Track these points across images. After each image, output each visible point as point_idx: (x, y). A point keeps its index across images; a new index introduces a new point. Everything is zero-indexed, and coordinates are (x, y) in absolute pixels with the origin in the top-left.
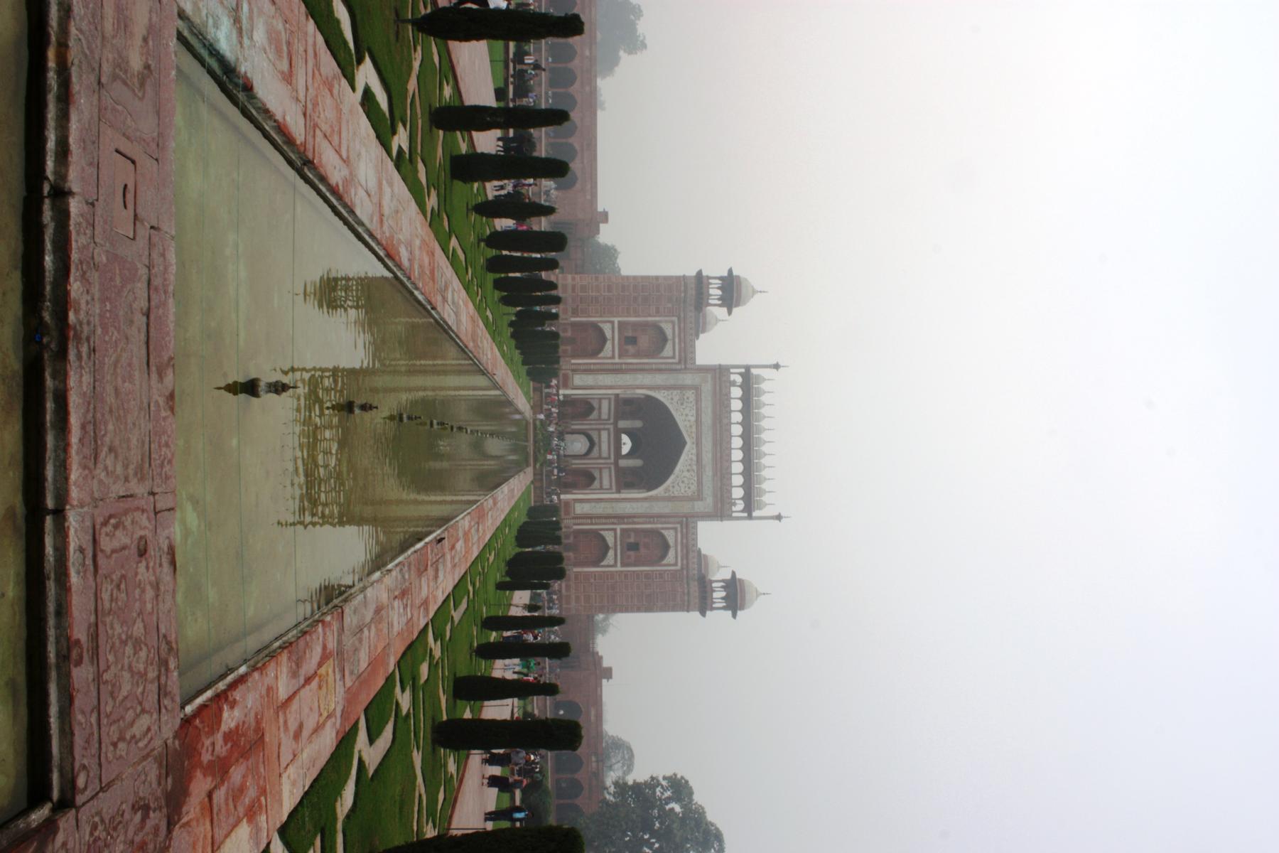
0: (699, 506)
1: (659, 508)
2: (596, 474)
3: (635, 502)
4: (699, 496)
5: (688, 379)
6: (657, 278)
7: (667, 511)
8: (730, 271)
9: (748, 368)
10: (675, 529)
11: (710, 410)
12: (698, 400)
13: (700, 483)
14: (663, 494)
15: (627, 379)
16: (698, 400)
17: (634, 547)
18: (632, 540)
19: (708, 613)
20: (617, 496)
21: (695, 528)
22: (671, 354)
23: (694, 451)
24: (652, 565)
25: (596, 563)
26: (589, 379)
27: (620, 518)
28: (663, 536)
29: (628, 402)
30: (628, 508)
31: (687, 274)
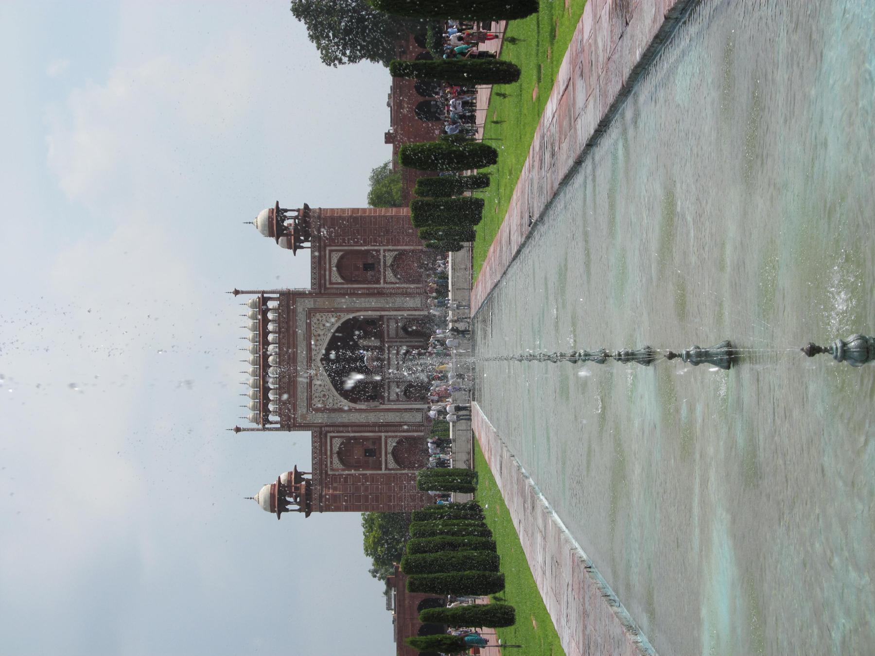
0: (309, 303)
1: (344, 302)
2: (401, 332)
3: (366, 307)
4: (310, 313)
5: (320, 418)
6: (347, 509)
7: (338, 300)
8: (279, 518)
9: (264, 429)
10: (331, 283)
11: (299, 389)
12: (310, 399)
13: (309, 325)
14: (342, 315)
15: (372, 418)
16: (310, 399)
17: (368, 267)
18: (370, 273)
19: (302, 207)
20: (383, 313)
21: (313, 284)
22: (334, 440)
23: (313, 353)
24: (352, 251)
25: (402, 253)
26: (407, 417)
27: (380, 293)
28: (342, 277)
29: (373, 398)
30: (373, 302)
31: (318, 513)
